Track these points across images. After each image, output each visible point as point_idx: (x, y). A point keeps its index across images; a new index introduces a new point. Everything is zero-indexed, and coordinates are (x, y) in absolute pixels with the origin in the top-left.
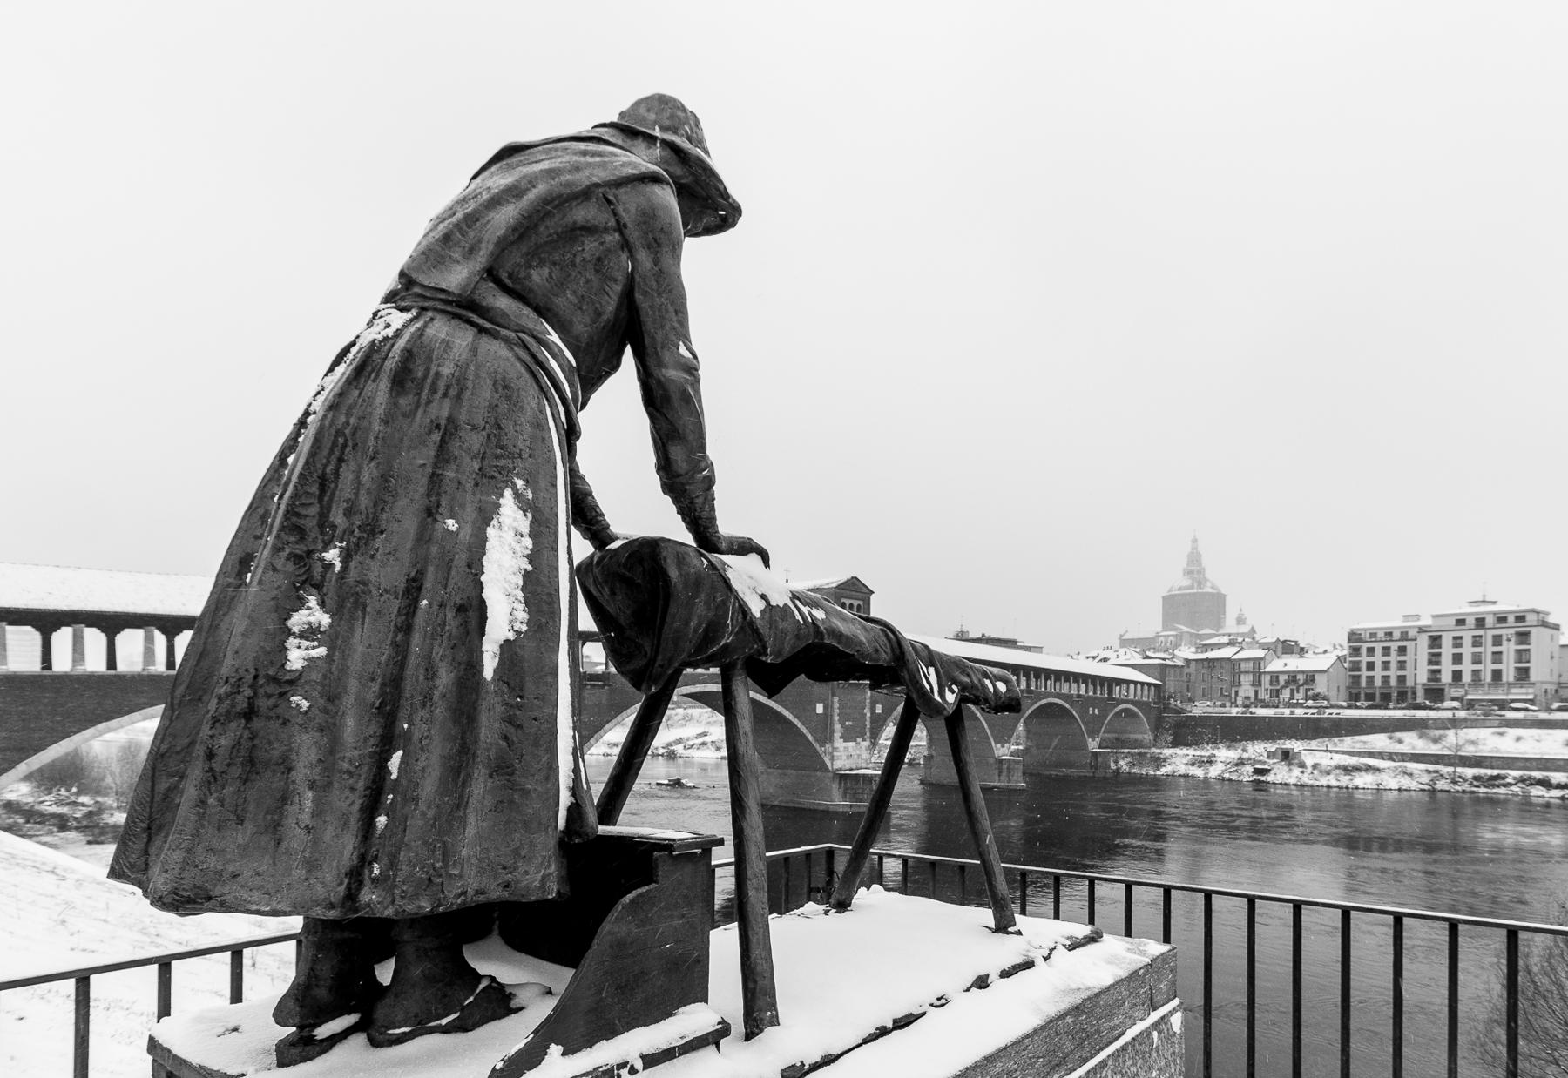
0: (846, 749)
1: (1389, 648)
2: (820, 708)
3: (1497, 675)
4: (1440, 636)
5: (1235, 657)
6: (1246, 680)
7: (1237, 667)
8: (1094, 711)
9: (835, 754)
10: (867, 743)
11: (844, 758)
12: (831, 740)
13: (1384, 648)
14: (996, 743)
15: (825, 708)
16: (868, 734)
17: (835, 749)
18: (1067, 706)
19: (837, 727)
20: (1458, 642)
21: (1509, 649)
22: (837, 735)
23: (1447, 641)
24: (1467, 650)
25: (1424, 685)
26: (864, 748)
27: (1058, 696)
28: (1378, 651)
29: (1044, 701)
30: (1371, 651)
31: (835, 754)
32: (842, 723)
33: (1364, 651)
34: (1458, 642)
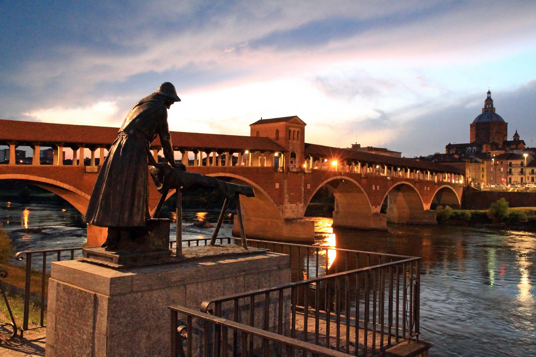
0: (291, 208)
2: (277, 186)
8: (427, 189)
9: (285, 210)
10: (302, 205)
11: (290, 212)
12: (282, 204)
14: (372, 206)
15: (280, 185)
16: (303, 200)
17: (286, 208)
18: (412, 186)
19: (287, 196)
22: (286, 200)
26: (300, 207)
27: (407, 180)
29: (399, 183)
31: (285, 210)
32: (289, 193)
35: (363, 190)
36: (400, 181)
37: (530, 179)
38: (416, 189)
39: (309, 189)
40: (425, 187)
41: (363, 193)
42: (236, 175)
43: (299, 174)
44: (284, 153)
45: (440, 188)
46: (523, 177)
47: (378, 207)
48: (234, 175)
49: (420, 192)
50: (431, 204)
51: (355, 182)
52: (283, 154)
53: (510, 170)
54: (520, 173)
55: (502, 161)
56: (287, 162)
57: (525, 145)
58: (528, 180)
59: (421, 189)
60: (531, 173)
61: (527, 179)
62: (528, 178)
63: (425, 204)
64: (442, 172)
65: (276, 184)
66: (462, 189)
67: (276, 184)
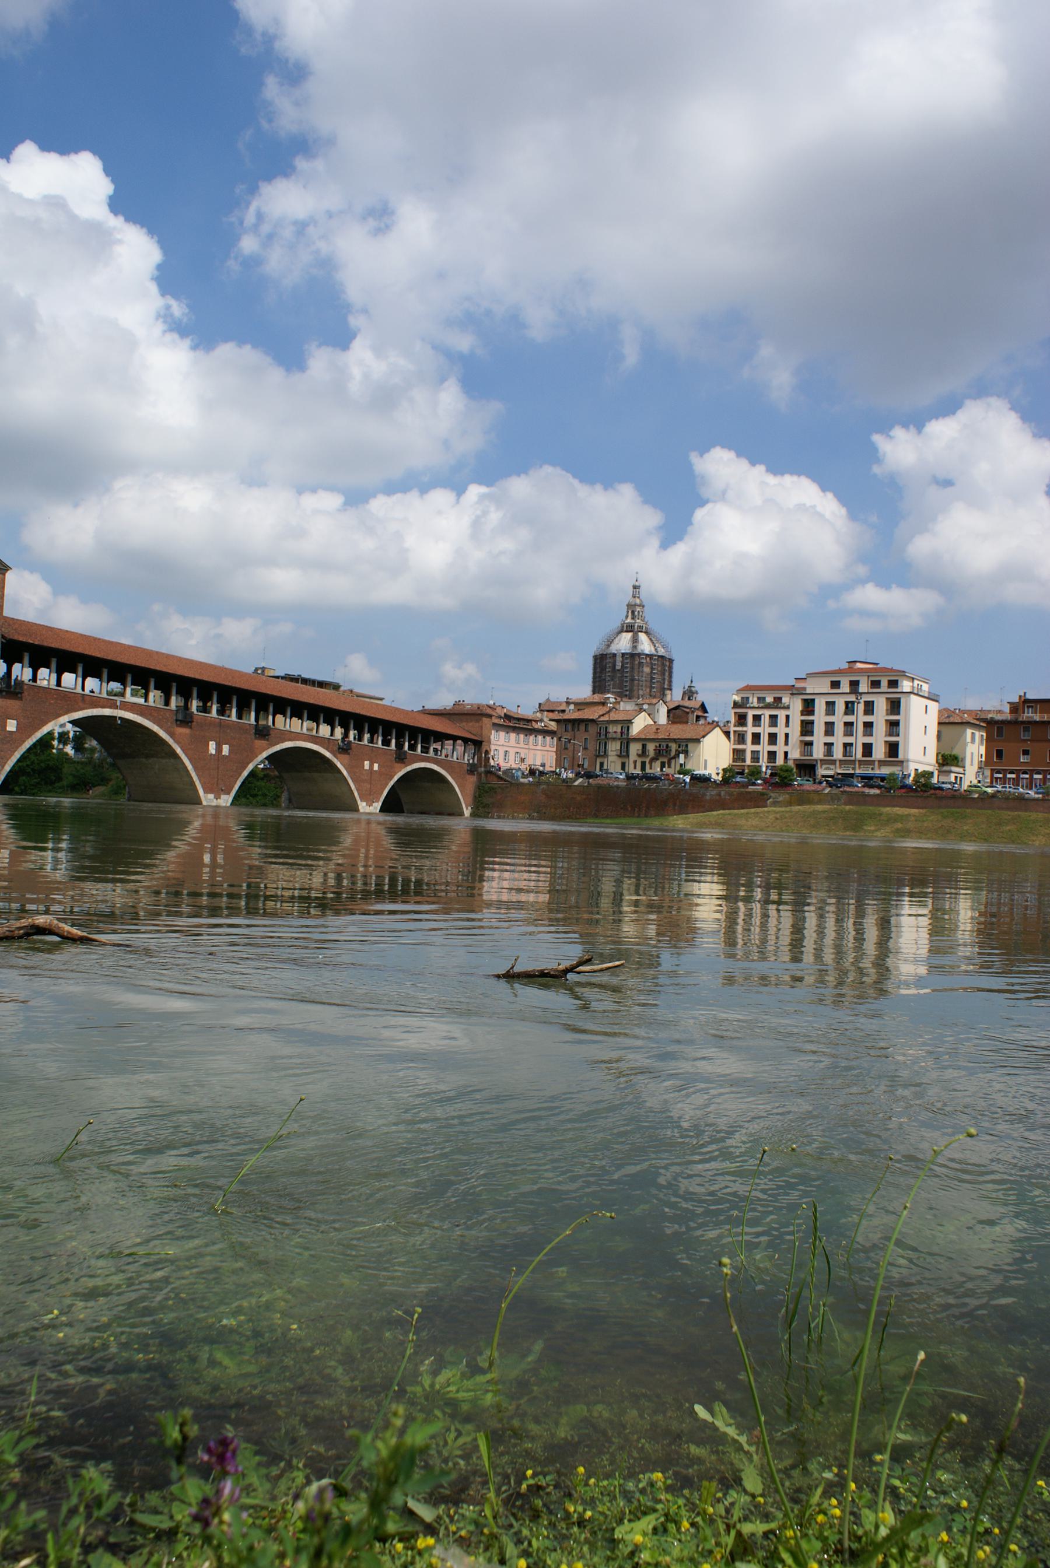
1: (776, 716)
3: (868, 749)
4: (813, 700)
5: (602, 719)
6: (614, 747)
7: (603, 732)
13: (771, 716)
14: (206, 792)
20: (830, 706)
21: (880, 716)
23: (820, 705)
24: (839, 718)
25: (795, 760)
28: (765, 720)
30: (757, 719)
33: (750, 720)
34: (830, 706)
35: (179, 751)
38: (339, 765)
39: (11, 733)
41: (179, 758)
45: (409, 768)
47: (223, 796)
49: (348, 772)
50: (380, 804)
51: (155, 728)
58: (635, 768)
59: (355, 768)
60: (640, 752)
61: (632, 765)
62: (635, 762)
63: (364, 804)
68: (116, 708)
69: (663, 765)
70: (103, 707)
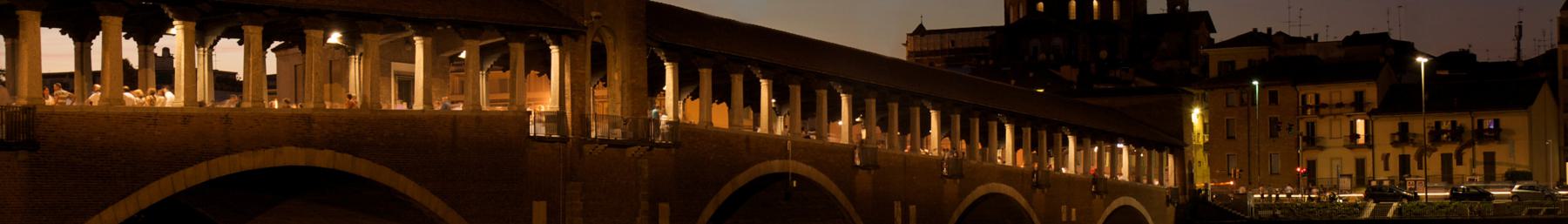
18: (1022, 201)
27: (1008, 174)
29: (981, 191)
36: (982, 182)
37: (1394, 163)
40: (1064, 208)
42: (358, 160)
43: (631, 151)
44: (565, 39)
45: (1108, 211)
46: (1368, 154)
48: (350, 156)
52: (558, 43)
53: (1311, 127)
54: (1348, 143)
55: (1273, 89)
56: (579, 92)
57: (1214, 31)
58: (1386, 168)
61: (1380, 164)
62: (1386, 158)
64: (1109, 138)
65: (535, 204)
66: (1171, 209)
67: (535, 204)
68: (787, 158)
69: (1446, 159)
70: (771, 158)
